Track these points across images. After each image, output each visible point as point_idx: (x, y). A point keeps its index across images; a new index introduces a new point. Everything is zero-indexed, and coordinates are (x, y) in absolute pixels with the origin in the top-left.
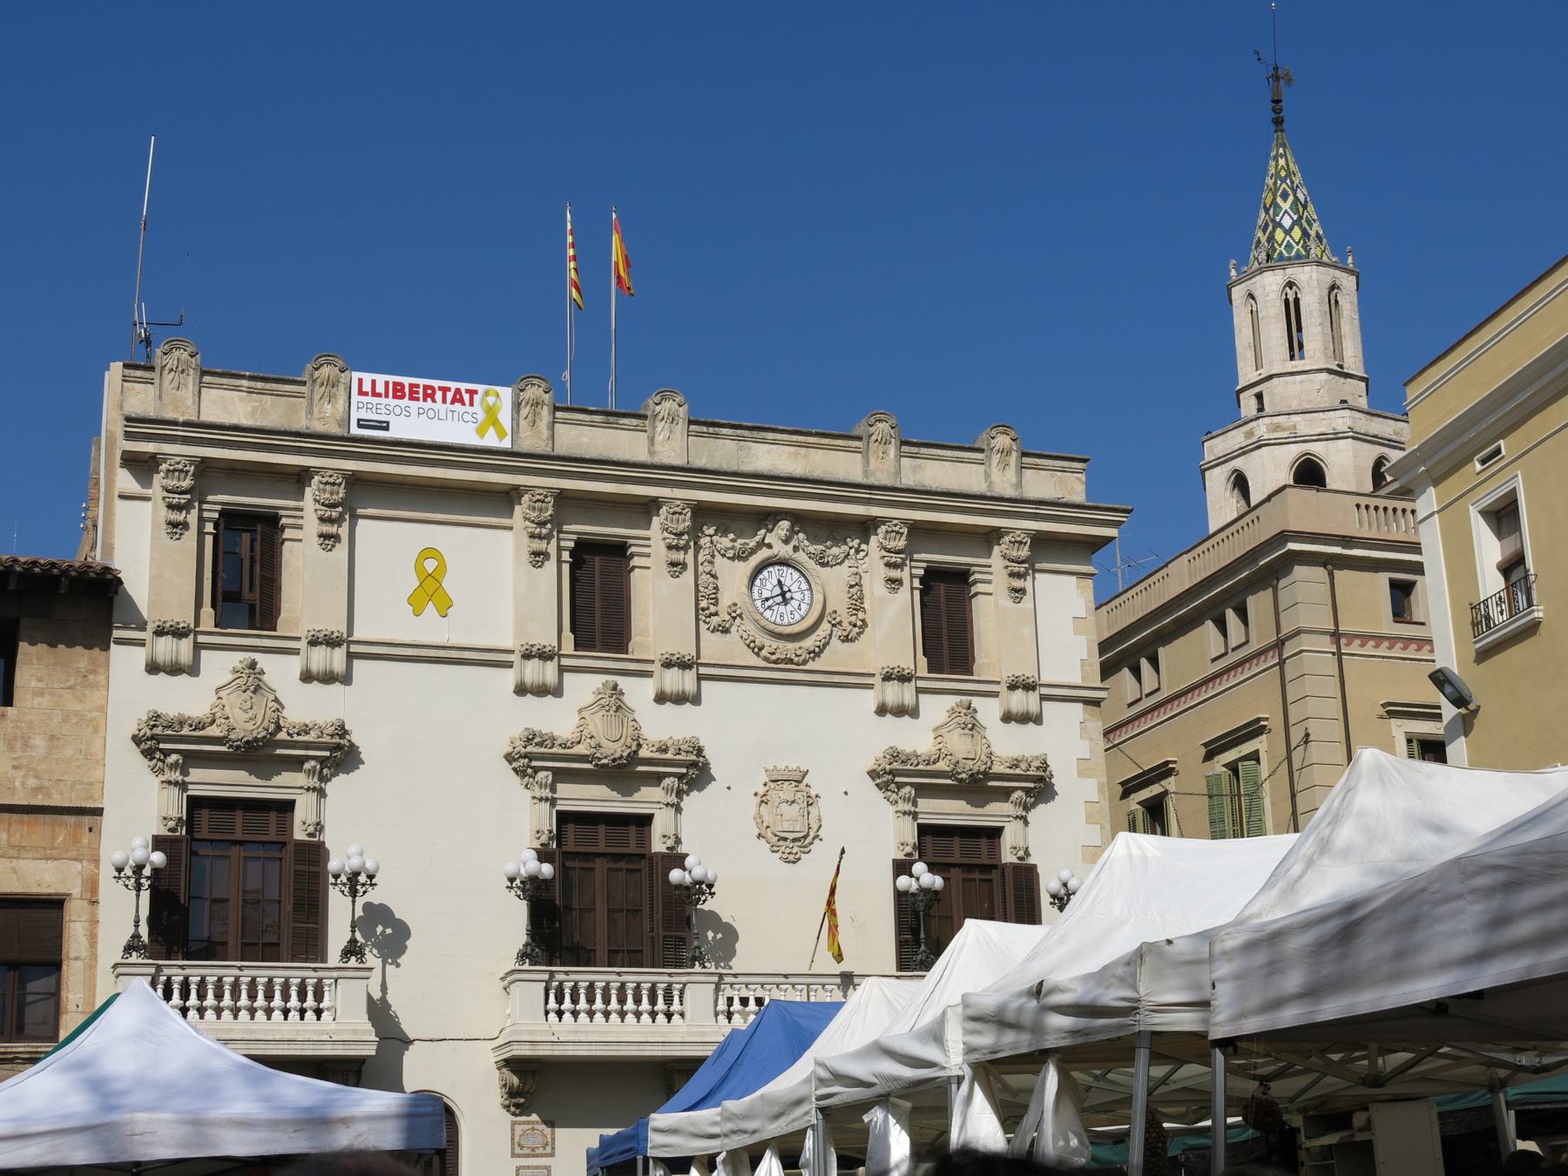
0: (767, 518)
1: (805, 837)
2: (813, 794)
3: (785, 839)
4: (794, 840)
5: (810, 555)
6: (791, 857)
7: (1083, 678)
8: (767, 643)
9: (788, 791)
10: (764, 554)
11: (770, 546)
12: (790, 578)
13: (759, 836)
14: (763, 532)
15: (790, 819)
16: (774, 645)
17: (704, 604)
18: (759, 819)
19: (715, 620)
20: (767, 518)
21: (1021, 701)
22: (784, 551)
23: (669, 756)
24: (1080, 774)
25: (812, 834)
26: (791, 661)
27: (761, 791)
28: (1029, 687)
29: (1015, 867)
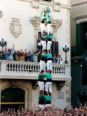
3: (16, 33)
21: (57, 8)
28: (59, 5)
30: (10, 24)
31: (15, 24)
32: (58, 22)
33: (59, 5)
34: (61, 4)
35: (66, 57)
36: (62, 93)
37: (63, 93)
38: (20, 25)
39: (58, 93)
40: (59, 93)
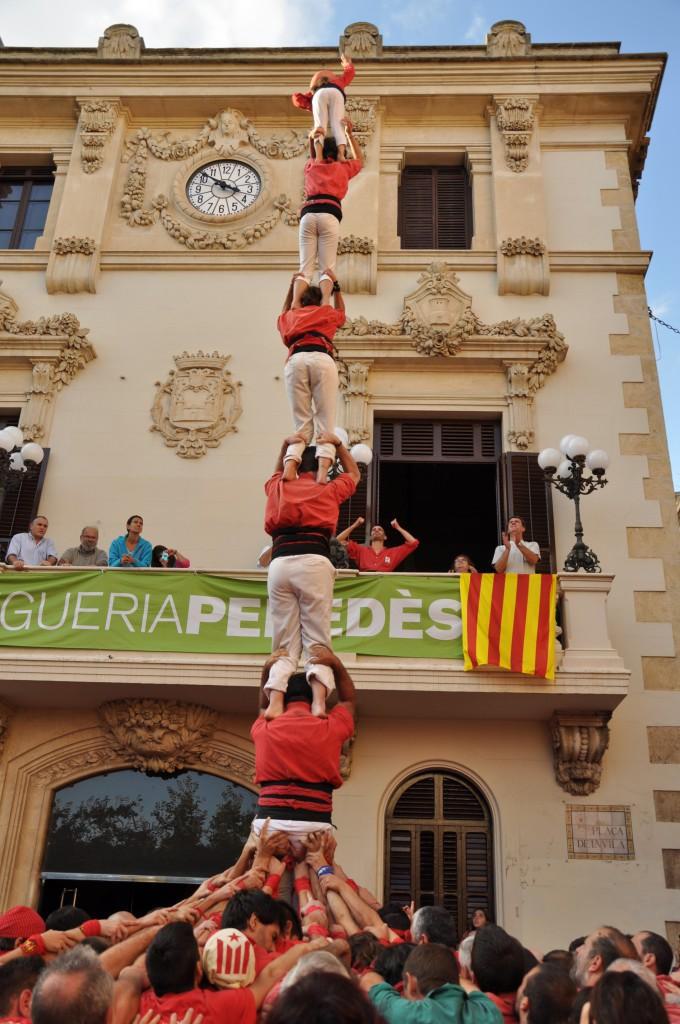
0: (209, 109)
1: (212, 428)
2: (234, 381)
3: (188, 430)
4: (199, 430)
5: (261, 150)
6: (192, 452)
7: (615, 248)
8: (193, 231)
9: (197, 378)
10: (207, 154)
11: (212, 144)
12: (235, 175)
13: (154, 429)
14: (207, 129)
15: (195, 406)
16: (204, 233)
17: (126, 198)
18: (156, 409)
19: (136, 215)
20: (209, 109)
21: (522, 269)
22: (226, 145)
23: (36, 336)
24: (614, 351)
25: (228, 425)
26: (224, 245)
27: (164, 379)
28: (536, 251)
29: (515, 457)
30: (155, 390)
31: (181, 382)
32: (518, 331)
33: (536, 251)
34: (548, 245)
35: (579, 523)
36: (619, 816)
37: (626, 811)
38: (229, 389)
39: (570, 810)
40: (584, 809)
